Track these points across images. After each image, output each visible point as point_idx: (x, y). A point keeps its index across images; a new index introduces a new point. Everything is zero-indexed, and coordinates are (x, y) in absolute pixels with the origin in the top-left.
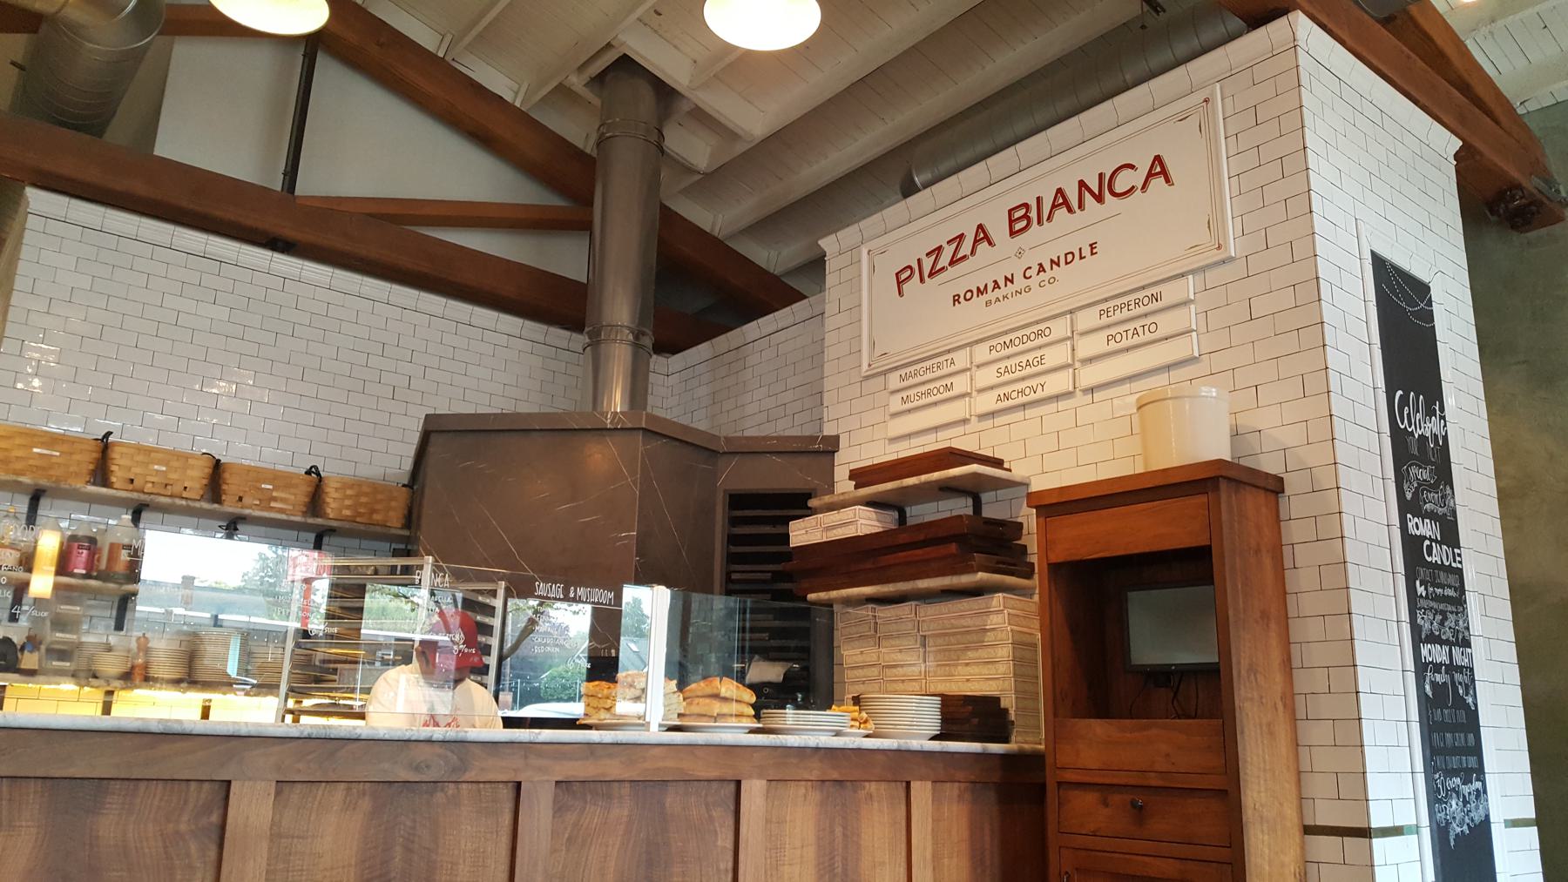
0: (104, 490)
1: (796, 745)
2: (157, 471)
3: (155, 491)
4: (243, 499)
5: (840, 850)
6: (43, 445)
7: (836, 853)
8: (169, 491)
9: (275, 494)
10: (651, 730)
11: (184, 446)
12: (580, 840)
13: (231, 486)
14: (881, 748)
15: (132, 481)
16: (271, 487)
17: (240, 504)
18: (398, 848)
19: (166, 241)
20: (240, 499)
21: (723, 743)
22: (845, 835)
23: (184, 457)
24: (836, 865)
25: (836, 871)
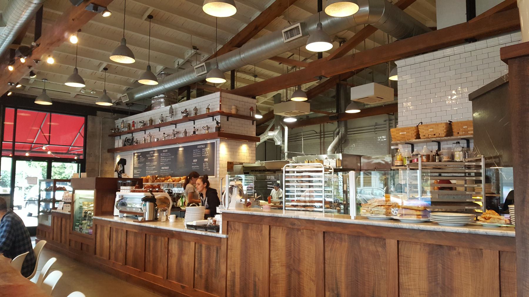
0: (419, 140)
1: (407, 228)
2: (431, 131)
3: (432, 137)
4: (459, 133)
5: (441, 273)
6: (402, 131)
7: (438, 274)
8: (435, 136)
9: (468, 129)
10: (352, 218)
11: (435, 120)
12: (334, 249)
13: (455, 129)
14: (457, 232)
15: (434, 135)
16: (466, 127)
17: (459, 135)
18: (292, 244)
19: (432, 58)
20: (458, 133)
21: (374, 225)
22: (443, 268)
23: (437, 125)
24: (439, 279)
25: (439, 282)
